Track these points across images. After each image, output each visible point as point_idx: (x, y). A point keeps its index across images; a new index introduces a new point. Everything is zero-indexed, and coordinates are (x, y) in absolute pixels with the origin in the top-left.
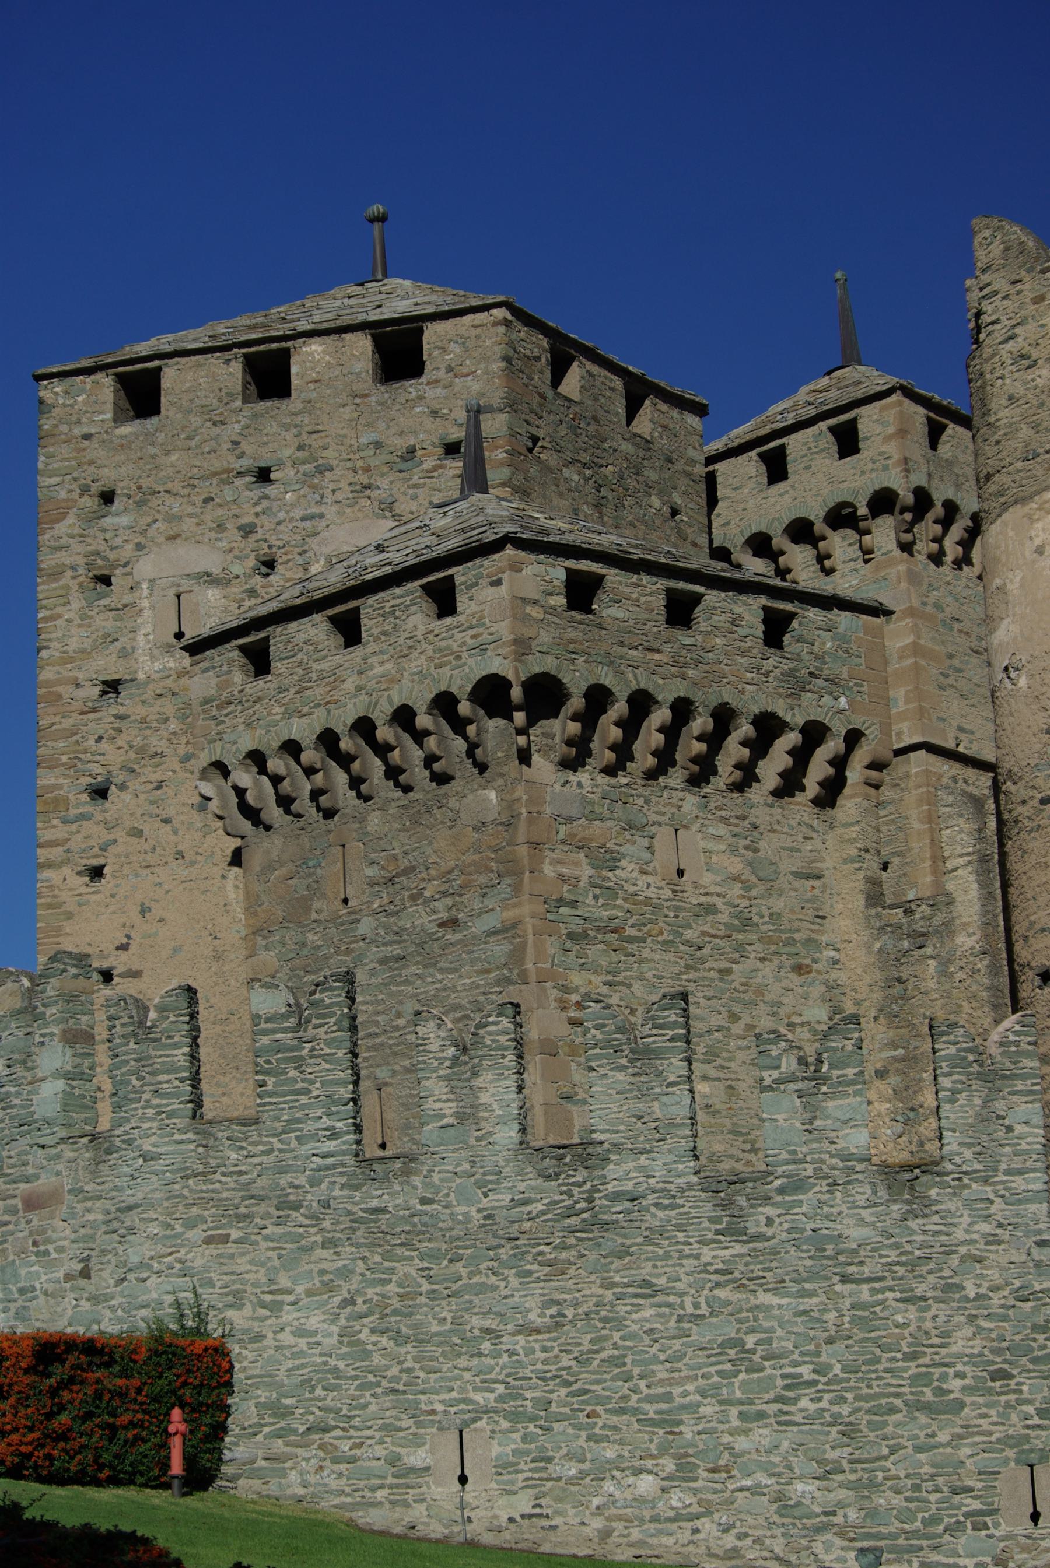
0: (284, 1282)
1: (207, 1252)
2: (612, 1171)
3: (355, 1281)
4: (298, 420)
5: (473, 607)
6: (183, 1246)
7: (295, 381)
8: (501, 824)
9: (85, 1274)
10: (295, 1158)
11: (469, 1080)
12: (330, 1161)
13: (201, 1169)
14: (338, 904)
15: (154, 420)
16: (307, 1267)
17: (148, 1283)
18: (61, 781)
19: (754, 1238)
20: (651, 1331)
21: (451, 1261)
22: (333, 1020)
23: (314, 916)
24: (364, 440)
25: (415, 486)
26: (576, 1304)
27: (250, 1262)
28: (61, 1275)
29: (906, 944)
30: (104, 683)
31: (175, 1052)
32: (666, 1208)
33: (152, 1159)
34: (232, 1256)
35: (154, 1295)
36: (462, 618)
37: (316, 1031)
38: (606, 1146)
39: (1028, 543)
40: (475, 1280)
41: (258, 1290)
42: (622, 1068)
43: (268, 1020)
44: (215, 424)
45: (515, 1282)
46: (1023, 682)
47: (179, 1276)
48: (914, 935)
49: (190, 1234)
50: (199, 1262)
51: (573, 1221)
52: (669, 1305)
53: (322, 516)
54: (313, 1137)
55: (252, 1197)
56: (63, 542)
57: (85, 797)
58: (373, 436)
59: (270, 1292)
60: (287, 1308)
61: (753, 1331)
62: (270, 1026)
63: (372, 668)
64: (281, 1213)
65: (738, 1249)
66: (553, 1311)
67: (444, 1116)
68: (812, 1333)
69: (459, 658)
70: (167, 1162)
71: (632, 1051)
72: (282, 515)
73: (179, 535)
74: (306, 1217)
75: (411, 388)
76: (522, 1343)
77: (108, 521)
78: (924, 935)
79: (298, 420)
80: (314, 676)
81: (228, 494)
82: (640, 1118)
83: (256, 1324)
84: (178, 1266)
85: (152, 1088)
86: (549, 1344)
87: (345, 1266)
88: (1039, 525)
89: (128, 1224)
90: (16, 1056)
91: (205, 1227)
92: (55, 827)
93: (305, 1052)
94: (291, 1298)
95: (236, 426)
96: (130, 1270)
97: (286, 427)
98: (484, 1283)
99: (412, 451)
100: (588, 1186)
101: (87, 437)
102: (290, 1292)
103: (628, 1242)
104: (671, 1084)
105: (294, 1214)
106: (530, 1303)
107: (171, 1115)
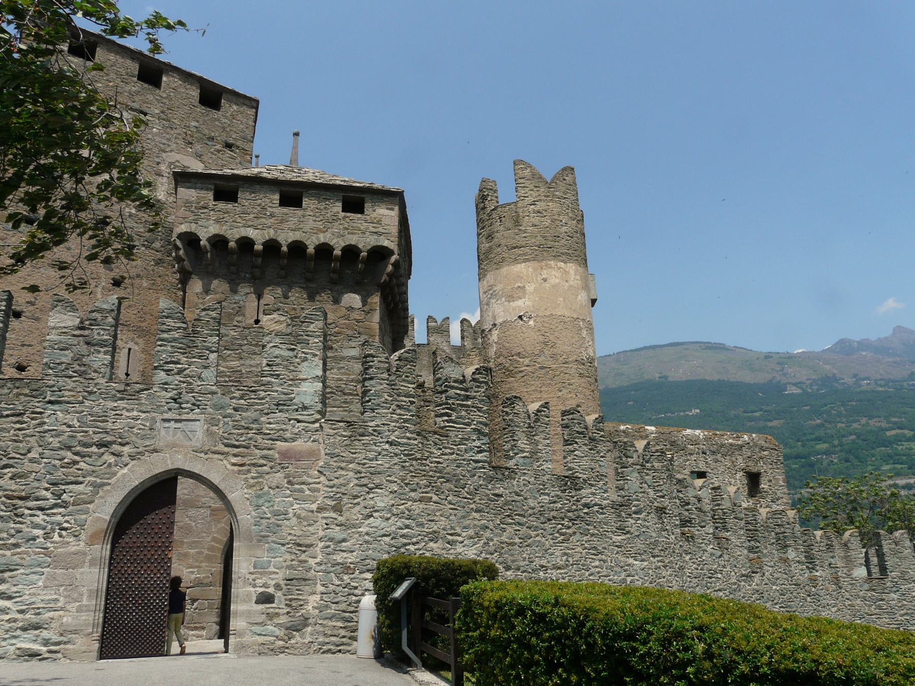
0: (458, 530)
1: (421, 506)
2: (584, 492)
3: (488, 534)
4: (164, 101)
5: (374, 215)
6: (408, 500)
7: (163, 84)
8: (363, 311)
9: (338, 509)
10: (464, 460)
11: (534, 436)
12: (480, 465)
13: (419, 456)
14: (252, 321)
16: (468, 522)
17: (390, 521)
19: (628, 532)
20: (599, 572)
21: (527, 527)
22: (483, 390)
23: (236, 323)
24: (194, 124)
25: (212, 153)
26: (572, 556)
27: (441, 515)
28: (314, 507)
29: (422, 403)
31: (409, 385)
32: (602, 513)
33: (395, 445)
34: (433, 511)
35: (393, 528)
36: (368, 218)
37: (475, 394)
38: (581, 480)
39: (539, 275)
40: (537, 538)
41: (445, 532)
42: (585, 445)
43: (455, 381)
44: (123, 82)
45: (552, 542)
46: (531, 323)
47: (407, 519)
48: (425, 401)
49: (413, 494)
50: (417, 512)
51: (570, 514)
52: (604, 561)
53: (169, 146)
54: (471, 449)
55: (443, 477)
58: (196, 124)
59: (451, 535)
60: (458, 544)
61: (629, 576)
62: (456, 385)
64: (457, 489)
65: (623, 537)
66: (564, 558)
67: (523, 451)
68: (646, 578)
69: (364, 233)
70: (403, 449)
71: (590, 438)
72: (150, 136)
74: (467, 493)
75: (214, 114)
76: (555, 574)
78: (429, 402)
79: (164, 101)
80: (268, 214)
82: (592, 469)
83: (444, 552)
84: (407, 512)
85: (397, 403)
86: (564, 575)
87: (485, 524)
88: (545, 271)
89: (377, 481)
90: (278, 361)
91: (420, 491)
93: (469, 403)
94: (460, 539)
96: (376, 511)
98: (539, 541)
99: (212, 139)
100: (575, 498)
102: (459, 535)
103: (589, 527)
104: (602, 457)
105: (463, 491)
106: (558, 553)
107: (406, 421)
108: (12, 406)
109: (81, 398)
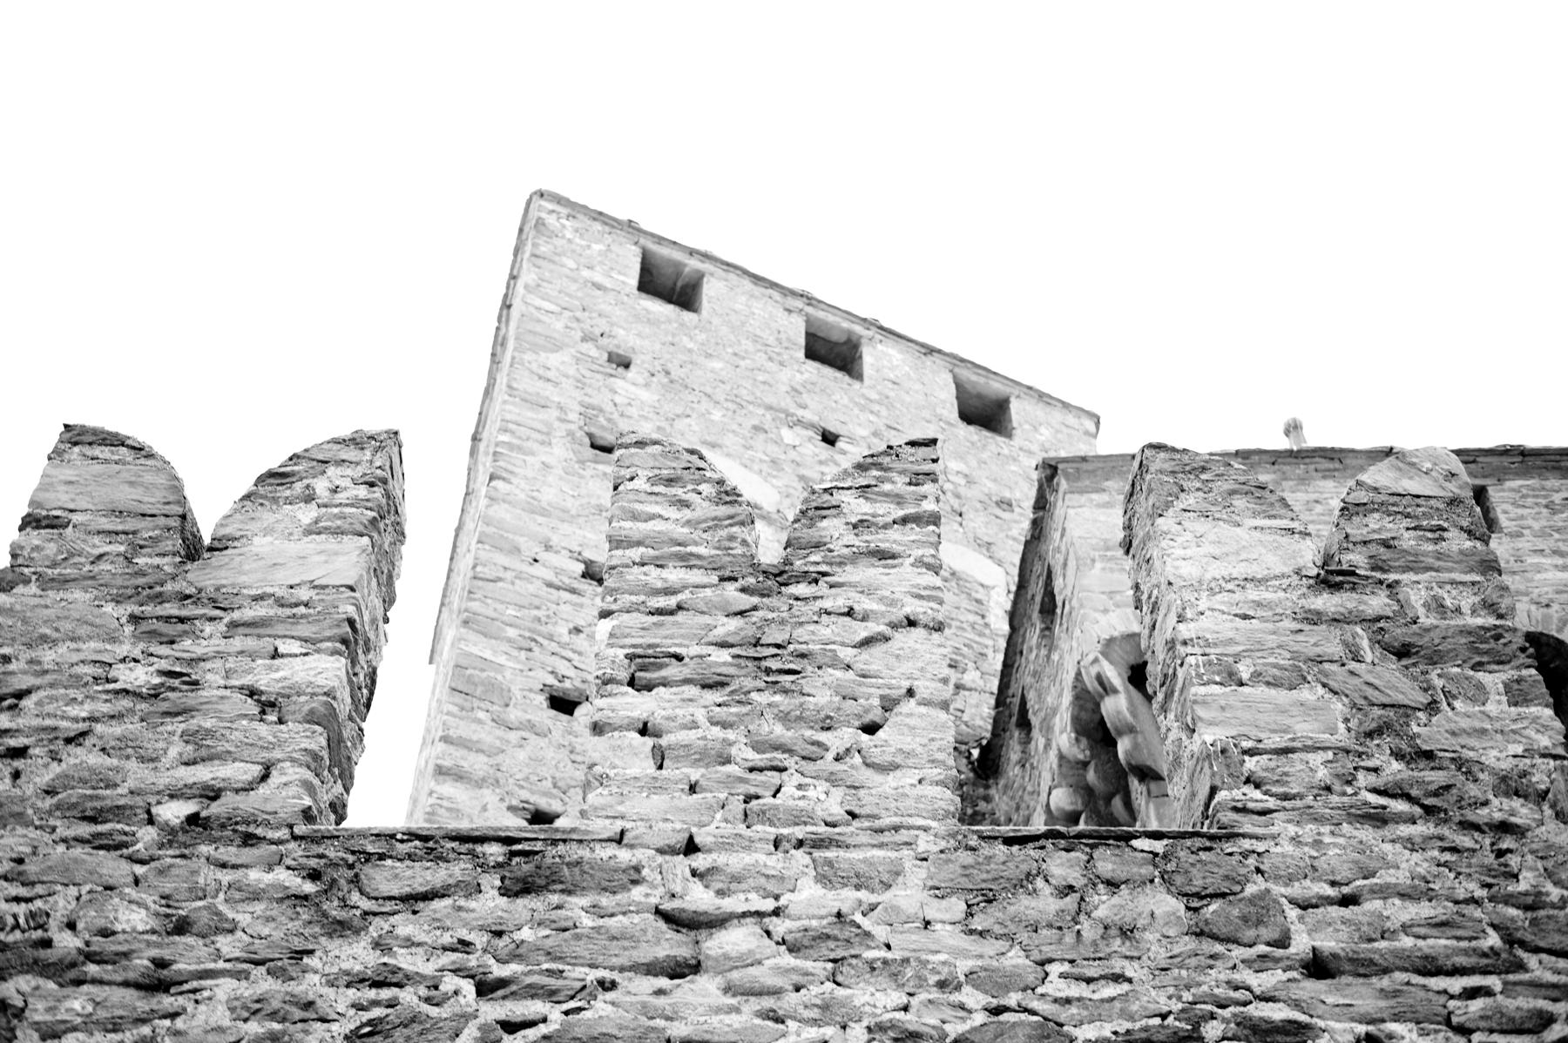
4: (876, 408)
15: (687, 316)
18: (502, 660)
30: (589, 564)
44: (770, 359)
56: (550, 374)
57: (541, 700)
63: (1539, 569)
73: (720, 446)
77: (618, 384)
79: (876, 408)
81: (788, 436)
92: (480, 722)
95: (798, 375)
97: (863, 409)
101: (599, 287)
108: (1110, 990)
109: (1493, 940)
